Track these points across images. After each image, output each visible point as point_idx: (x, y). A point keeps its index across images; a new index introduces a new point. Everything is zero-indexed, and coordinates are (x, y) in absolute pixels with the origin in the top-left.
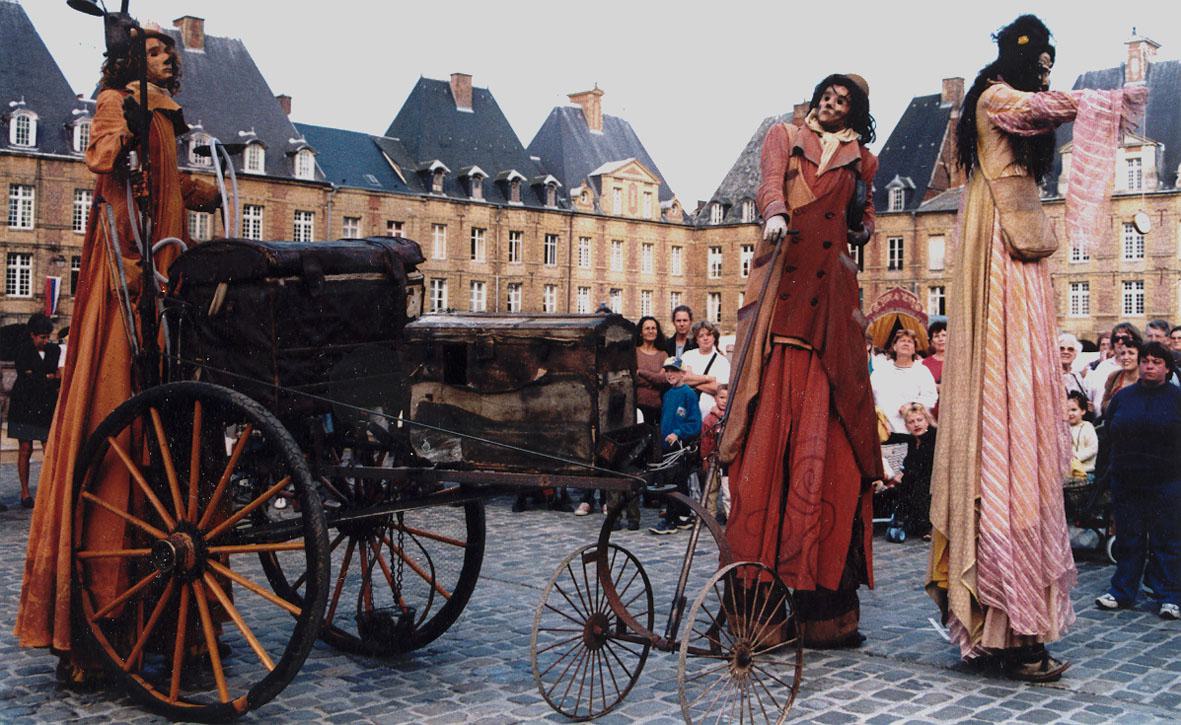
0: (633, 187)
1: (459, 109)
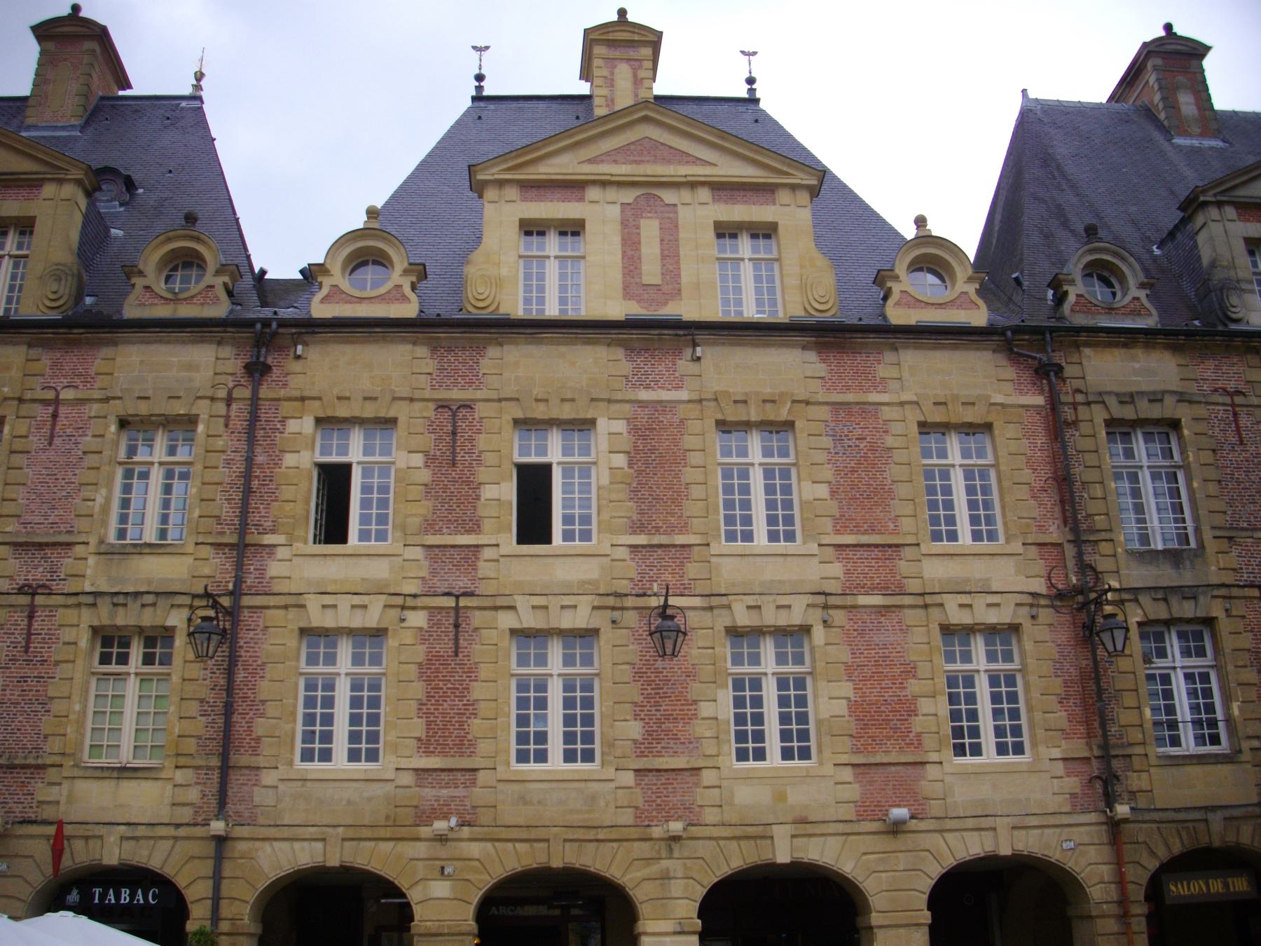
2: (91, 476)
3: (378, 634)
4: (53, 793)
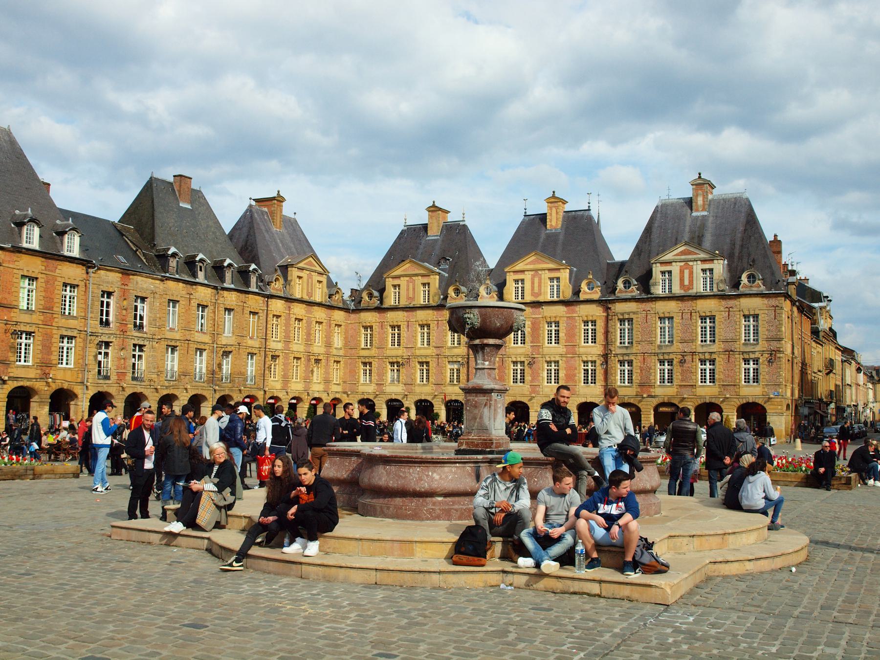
0: (310, 277)
1: (181, 205)
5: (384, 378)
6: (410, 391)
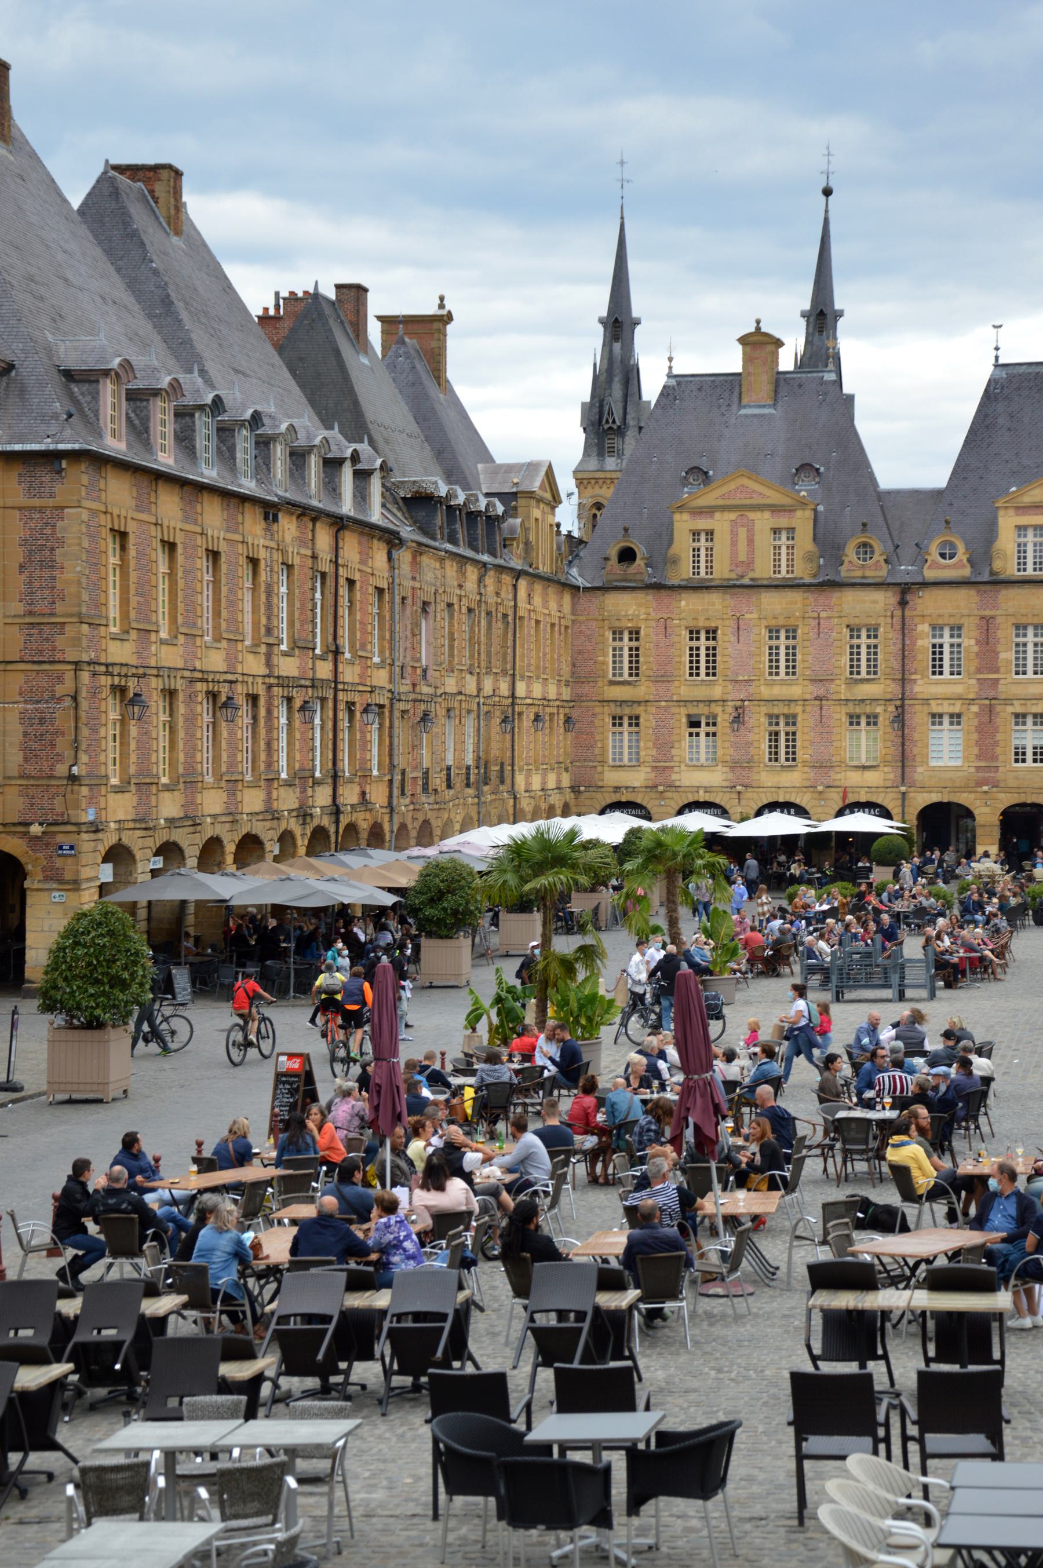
2: (838, 651)
3: (959, 716)
4: (839, 776)
5: (674, 752)
6: (746, 782)
